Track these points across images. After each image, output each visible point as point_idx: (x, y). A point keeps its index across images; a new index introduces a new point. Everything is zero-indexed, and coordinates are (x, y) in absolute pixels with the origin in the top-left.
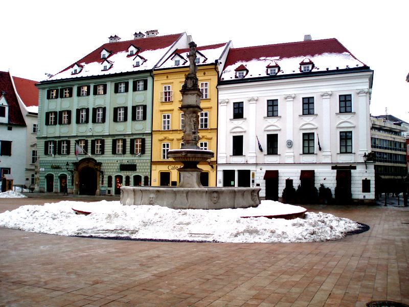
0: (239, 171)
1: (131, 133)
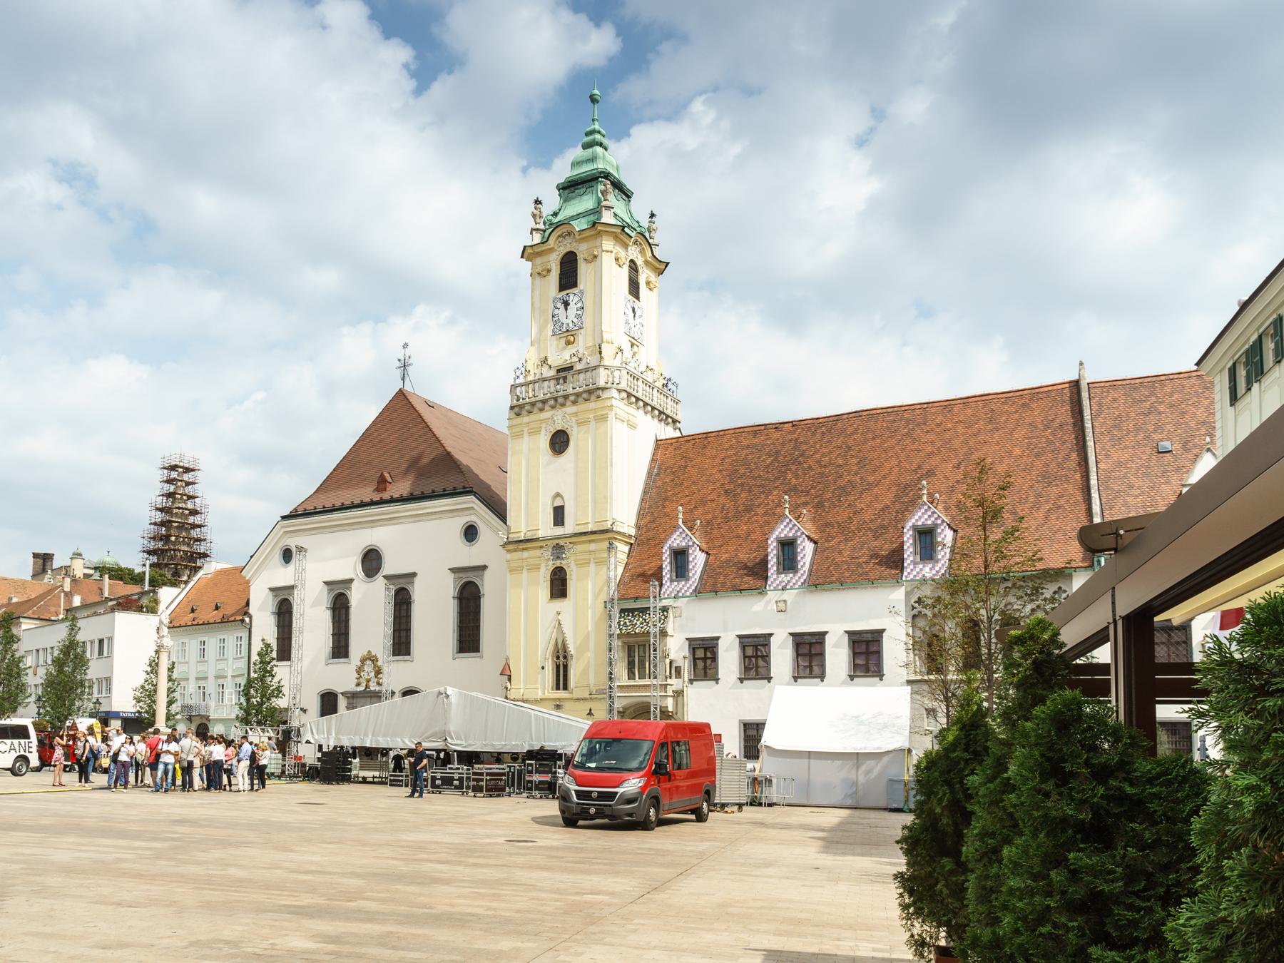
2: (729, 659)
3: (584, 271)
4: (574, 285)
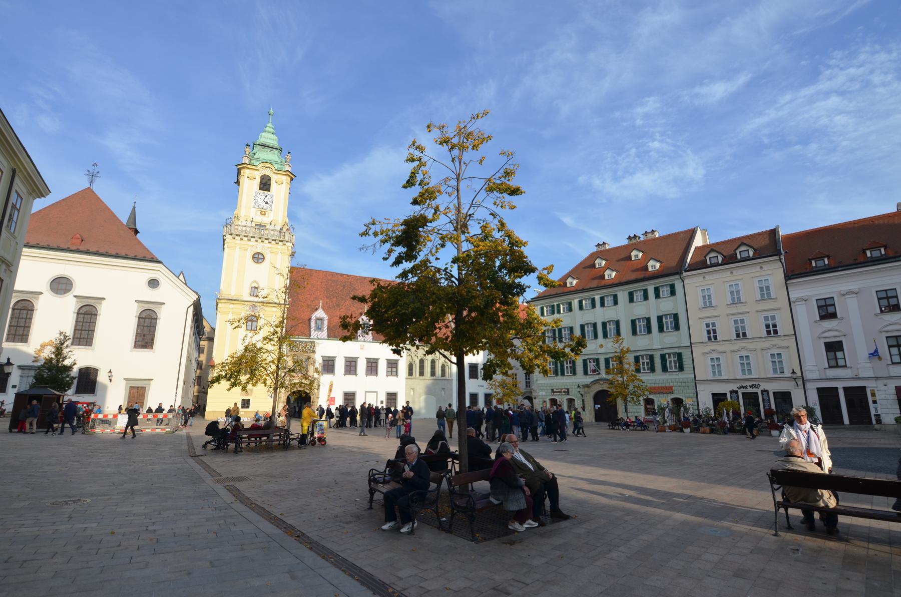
0: (845, 389)
1: (659, 347)
2: (340, 366)
3: (273, 185)
4: (269, 190)
